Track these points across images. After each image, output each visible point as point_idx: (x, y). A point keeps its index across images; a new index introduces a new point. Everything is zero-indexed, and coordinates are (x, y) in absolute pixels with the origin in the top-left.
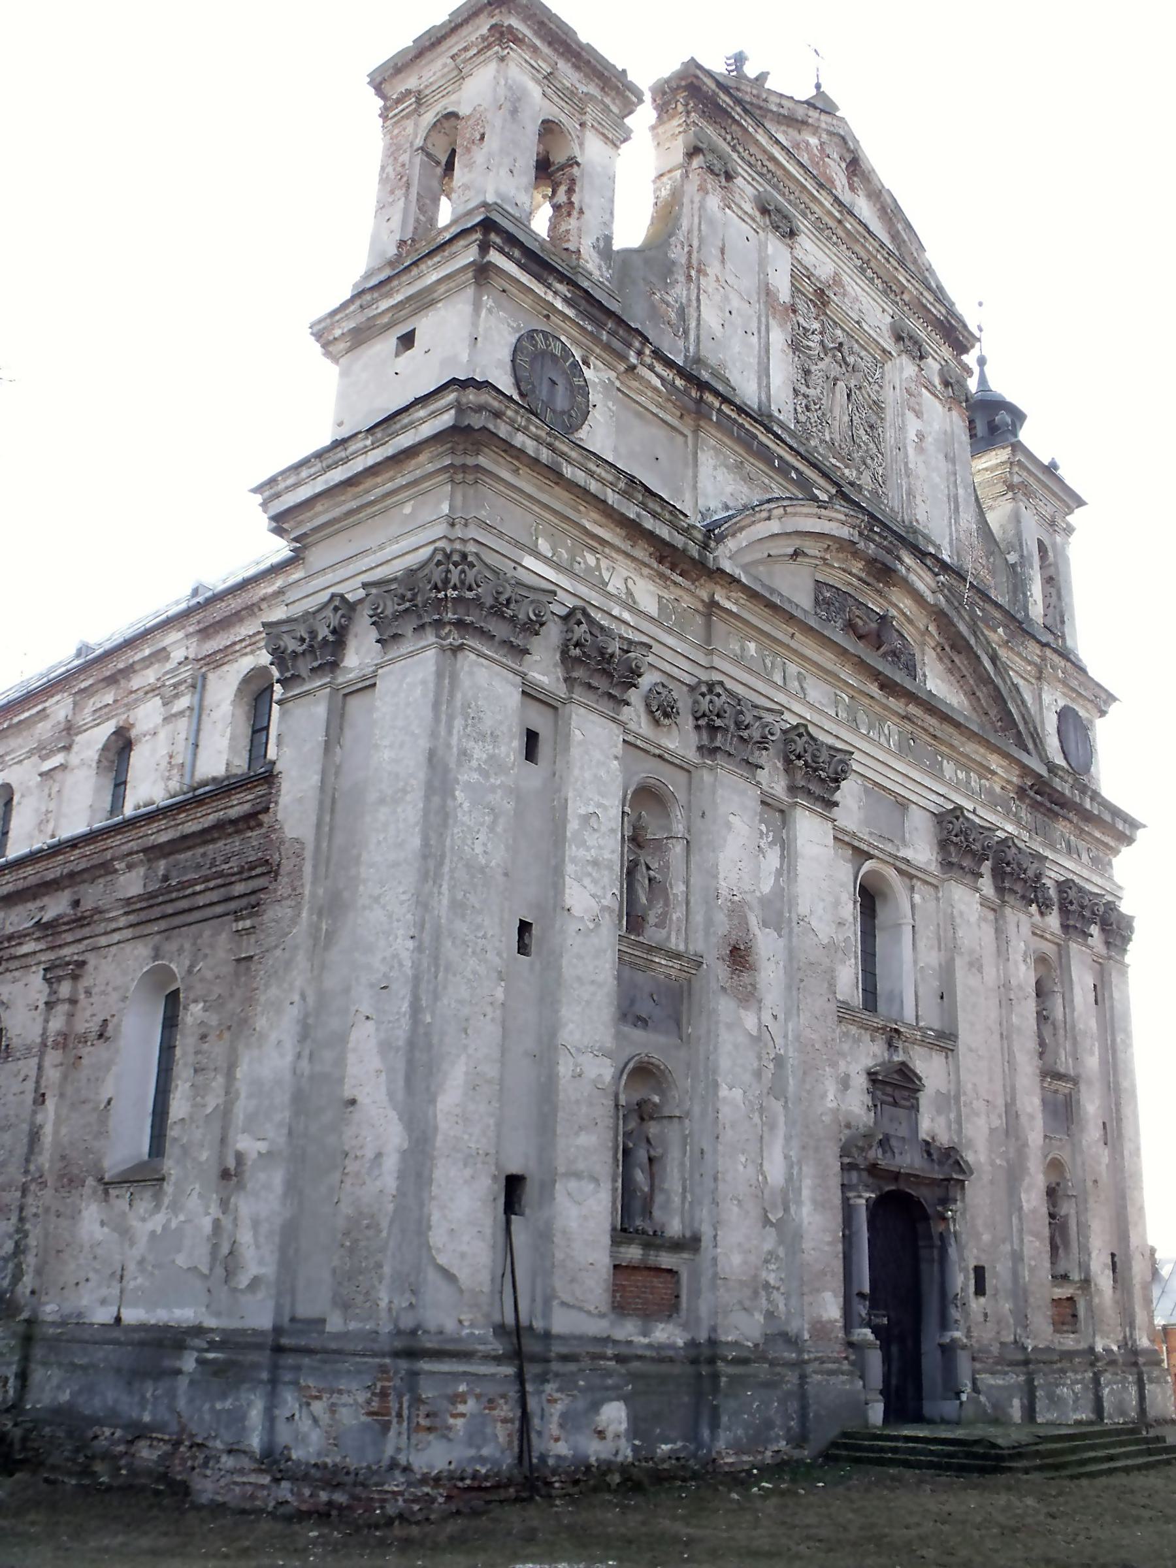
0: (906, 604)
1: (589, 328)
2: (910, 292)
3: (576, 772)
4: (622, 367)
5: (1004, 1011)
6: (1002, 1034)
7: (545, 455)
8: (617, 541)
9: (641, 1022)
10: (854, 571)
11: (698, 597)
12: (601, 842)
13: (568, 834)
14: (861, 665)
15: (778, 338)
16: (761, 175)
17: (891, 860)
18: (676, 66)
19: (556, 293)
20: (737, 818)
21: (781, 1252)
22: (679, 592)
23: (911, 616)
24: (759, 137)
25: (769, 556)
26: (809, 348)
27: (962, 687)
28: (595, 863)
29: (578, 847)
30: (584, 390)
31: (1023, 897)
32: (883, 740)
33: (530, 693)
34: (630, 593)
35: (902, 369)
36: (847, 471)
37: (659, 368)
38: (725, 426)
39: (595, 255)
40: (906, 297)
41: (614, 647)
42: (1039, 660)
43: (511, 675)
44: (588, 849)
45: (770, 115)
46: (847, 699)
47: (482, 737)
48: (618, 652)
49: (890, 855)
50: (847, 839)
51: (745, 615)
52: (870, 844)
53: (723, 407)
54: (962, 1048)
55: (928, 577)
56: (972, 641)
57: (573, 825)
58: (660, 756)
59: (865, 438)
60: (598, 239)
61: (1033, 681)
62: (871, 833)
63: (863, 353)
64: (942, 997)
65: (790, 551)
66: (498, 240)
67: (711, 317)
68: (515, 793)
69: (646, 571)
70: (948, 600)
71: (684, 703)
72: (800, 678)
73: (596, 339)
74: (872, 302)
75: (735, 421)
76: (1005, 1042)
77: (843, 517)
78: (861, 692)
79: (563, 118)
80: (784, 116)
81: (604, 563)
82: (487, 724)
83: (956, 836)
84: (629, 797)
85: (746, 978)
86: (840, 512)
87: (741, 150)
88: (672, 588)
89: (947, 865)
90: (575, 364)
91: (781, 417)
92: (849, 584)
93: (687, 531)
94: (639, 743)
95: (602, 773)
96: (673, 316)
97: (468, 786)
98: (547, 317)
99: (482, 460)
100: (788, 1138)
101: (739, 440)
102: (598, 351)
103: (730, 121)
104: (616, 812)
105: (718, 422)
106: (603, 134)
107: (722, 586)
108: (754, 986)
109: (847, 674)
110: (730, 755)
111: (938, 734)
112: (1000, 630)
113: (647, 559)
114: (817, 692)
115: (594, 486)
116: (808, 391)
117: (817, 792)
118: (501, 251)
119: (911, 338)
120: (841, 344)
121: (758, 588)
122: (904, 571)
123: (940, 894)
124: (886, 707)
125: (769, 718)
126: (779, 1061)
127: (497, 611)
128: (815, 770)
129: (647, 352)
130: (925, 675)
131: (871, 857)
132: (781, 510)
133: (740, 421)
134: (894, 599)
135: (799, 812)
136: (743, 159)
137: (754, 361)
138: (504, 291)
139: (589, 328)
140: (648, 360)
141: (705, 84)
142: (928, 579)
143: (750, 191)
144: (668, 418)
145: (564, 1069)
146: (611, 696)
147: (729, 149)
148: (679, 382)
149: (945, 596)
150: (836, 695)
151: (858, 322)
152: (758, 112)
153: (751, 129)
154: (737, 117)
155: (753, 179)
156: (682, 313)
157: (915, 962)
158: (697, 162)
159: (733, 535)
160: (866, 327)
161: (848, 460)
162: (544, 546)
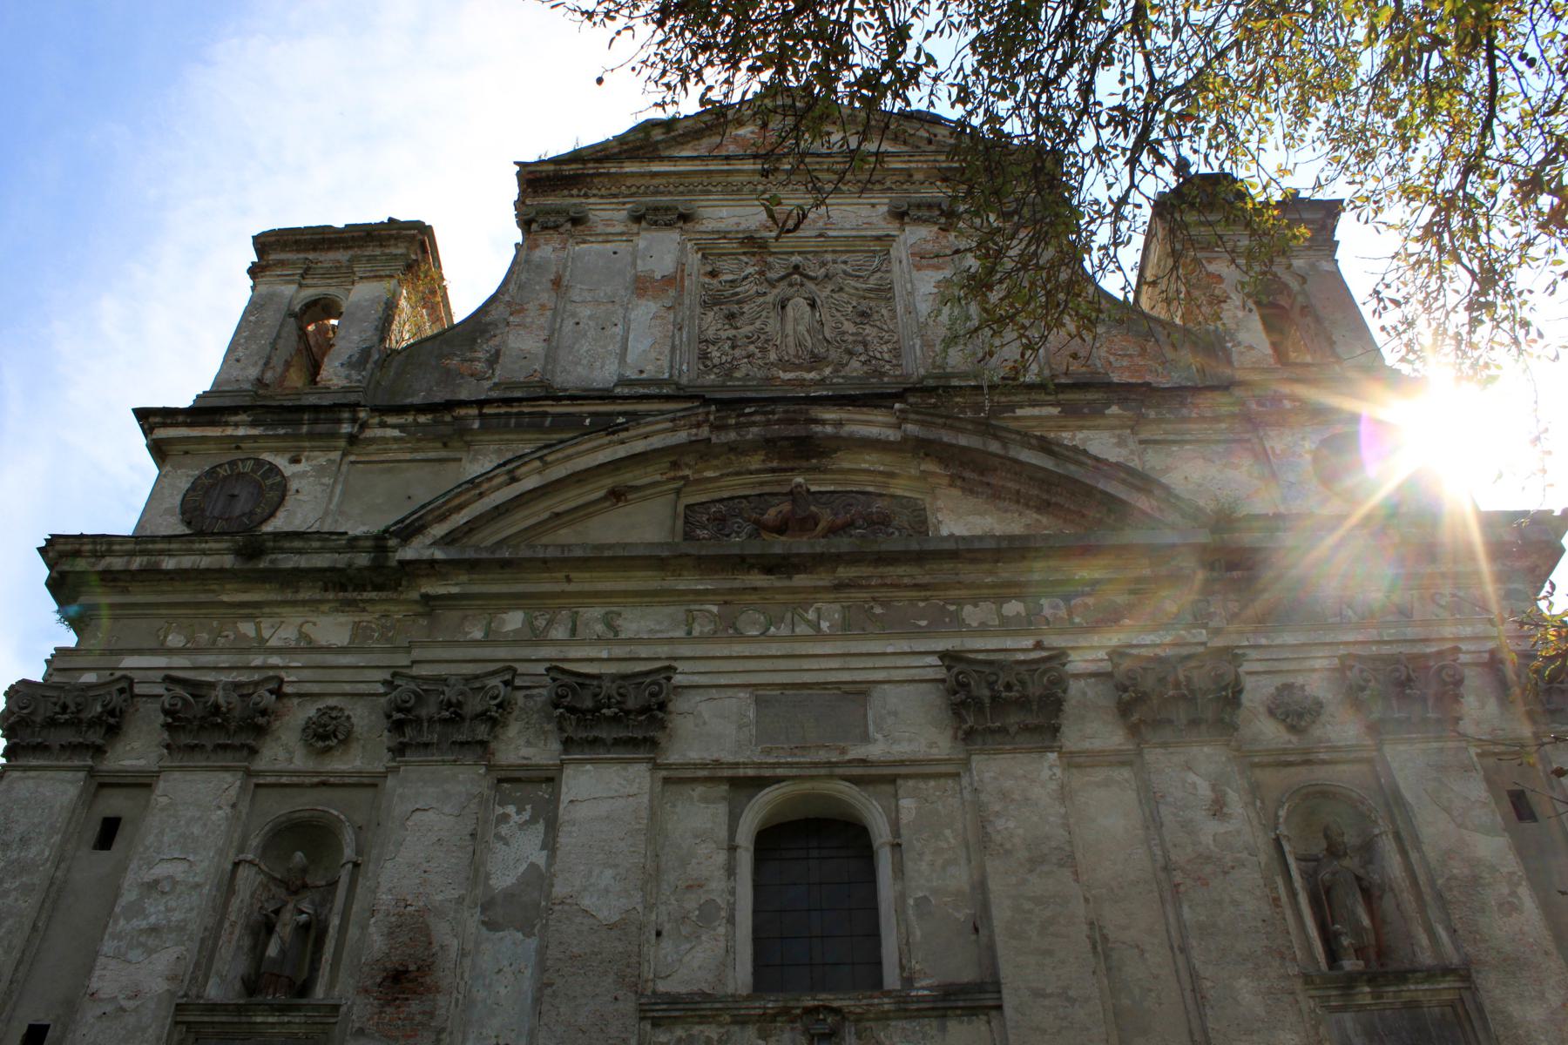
1: (281, 431)
2: (917, 169)
3: (151, 839)
4: (342, 443)
5: (1169, 908)
6: (1172, 948)
7: (137, 563)
8: (272, 596)
10: (753, 467)
11: (406, 602)
12: (173, 904)
13: (117, 910)
16: (632, 195)
17: (823, 771)
18: (515, 178)
19: (236, 425)
20: (430, 813)
23: (887, 469)
24: (627, 170)
25: (557, 515)
26: (737, 294)
27: (1027, 505)
28: (154, 930)
29: (128, 920)
31: (1194, 723)
32: (801, 629)
33: (101, 784)
34: (303, 635)
35: (905, 243)
36: (812, 375)
37: (391, 420)
39: (343, 372)
40: (918, 177)
41: (219, 696)
42: (1236, 409)
43: (70, 775)
44: (146, 917)
45: (660, 146)
46: (715, 609)
48: (221, 701)
49: (815, 765)
50: (705, 773)
51: (475, 589)
52: (760, 765)
53: (485, 411)
54: (1009, 1001)
55: (880, 416)
56: (995, 447)
57: (129, 895)
58: (324, 784)
60: (350, 357)
61: (1247, 436)
62: (768, 752)
63: (844, 257)
64: (976, 930)
65: (602, 493)
66: (157, 420)
69: (325, 608)
70: (922, 423)
71: (363, 718)
73: (297, 437)
74: (848, 208)
75: (506, 414)
76: (1180, 958)
77: (669, 425)
78: (731, 591)
79: (332, 291)
80: (680, 135)
81: (265, 624)
83: (955, 693)
84: (255, 842)
85: (414, 1006)
86: (657, 423)
87: (595, 192)
88: (369, 608)
89: (969, 736)
90: (274, 469)
91: (644, 376)
92: (762, 484)
93: (353, 543)
94: (284, 780)
95: (196, 830)
98: (238, 448)
101: (519, 428)
102: (307, 444)
103: (588, 179)
104: (205, 864)
105: (482, 426)
106: (376, 277)
107: (427, 575)
108: (431, 1014)
110: (426, 745)
111: (926, 579)
113: (318, 596)
114: (635, 623)
115: (205, 562)
116: (731, 333)
117: (640, 737)
118: (164, 425)
119: (919, 206)
120: (796, 268)
121: (470, 554)
122: (829, 429)
123: (965, 781)
124: (793, 591)
127: (52, 723)
128: (598, 709)
129: (362, 415)
130: (940, 522)
131: (778, 780)
132: (537, 464)
133: (515, 410)
134: (846, 465)
135: (569, 771)
136: (602, 197)
137: (615, 347)
138: (186, 453)
139: (281, 431)
140: (376, 420)
141: (541, 172)
142: (880, 418)
144: (432, 455)
146: (225, 747)
147: (584, 200)
148: (422, 419)
149: (915, 422)
150: (691, 611)
151: (820, 235)
152: (641, 152)
153: (613, 170)
154: (591, 171)
155: (624, 204)
157: (901, 897)
158: (534, 227)
159: (442, 518)
160: (831, 233)
161: (816, 361)
162: (175, 640)
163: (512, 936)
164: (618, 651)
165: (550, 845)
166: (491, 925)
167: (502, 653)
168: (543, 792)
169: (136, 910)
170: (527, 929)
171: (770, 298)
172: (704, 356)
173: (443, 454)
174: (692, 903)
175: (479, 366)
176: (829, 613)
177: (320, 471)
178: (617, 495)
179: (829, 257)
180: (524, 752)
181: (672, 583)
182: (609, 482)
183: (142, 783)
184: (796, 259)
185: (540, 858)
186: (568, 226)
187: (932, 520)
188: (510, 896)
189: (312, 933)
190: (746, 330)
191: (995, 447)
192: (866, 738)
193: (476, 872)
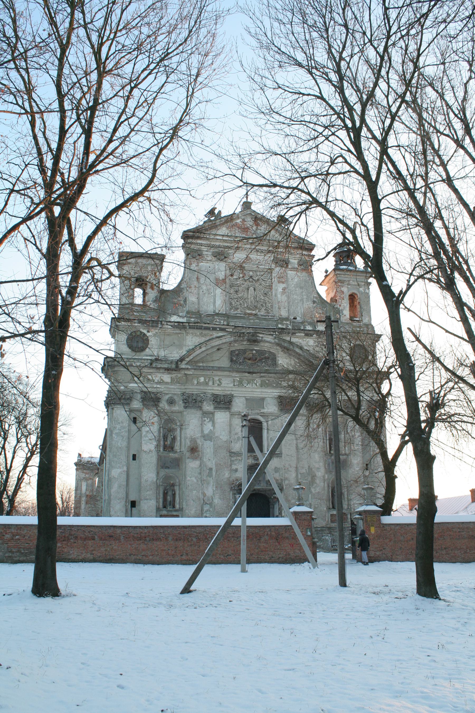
0: (267, 344)
9: (169, 468)
14: (237, 372)
15: (219, 291)
21: (211, 509)
22: (175, 375)
30: (147, 340)
32: (254, 385)
33: (131, 411)
34: (162, 380)
36: (254, 312)
38: (190, 327)
41: (153, 396)
47: (119, 423)
54: (283, 456)
55: (271, 337)
56: (291, 347)
59: (263, 298)
67: (192, 298)
68: (129, 431)
72: (219, 380)
82: (120, 420)
85: (196, 454)
89: (281, 410)
90: (145, 334)
96: (182, 302)
97: (116, 433)
99: (116, 369)
100: (213, 485)
101: (197, 328)
108: (199, 455)
109: (234, 374)
112: (315, 335)
125: (202, 395)
126: (211, 469)
135: (216, 413)
143: (210, 253)
145: (143, 480)
148: (176, 324)
156: (185, 301)
157: (268, 437)
161: (256, 307)
163: (209, 442)
164: (222, 389)
165: (214, 425)
166: (205, 440)
167: (202, 388)
168: (211, 416)
169: (146, 436)
170: (211, 440)
171: (245, 285)
172: (231, 304)
173: (180, 332)
174: (236, 437)
175: (182, 302)
176: (258, 381)
177: (155, 335)
178: (218, 349)
179: (258, 273)
180: (207, 408)
181: (231, 374)
182: (217, 347)
183: (140, 411)
184: (251, 273)
185: (212, 428)
186: (198, 257)
187: (277, 359)
188: (208, 435)
189: (174, 439)
190: (240, 295)
191: (291, 347)
192: (263, 408)
193: (202, 431)
